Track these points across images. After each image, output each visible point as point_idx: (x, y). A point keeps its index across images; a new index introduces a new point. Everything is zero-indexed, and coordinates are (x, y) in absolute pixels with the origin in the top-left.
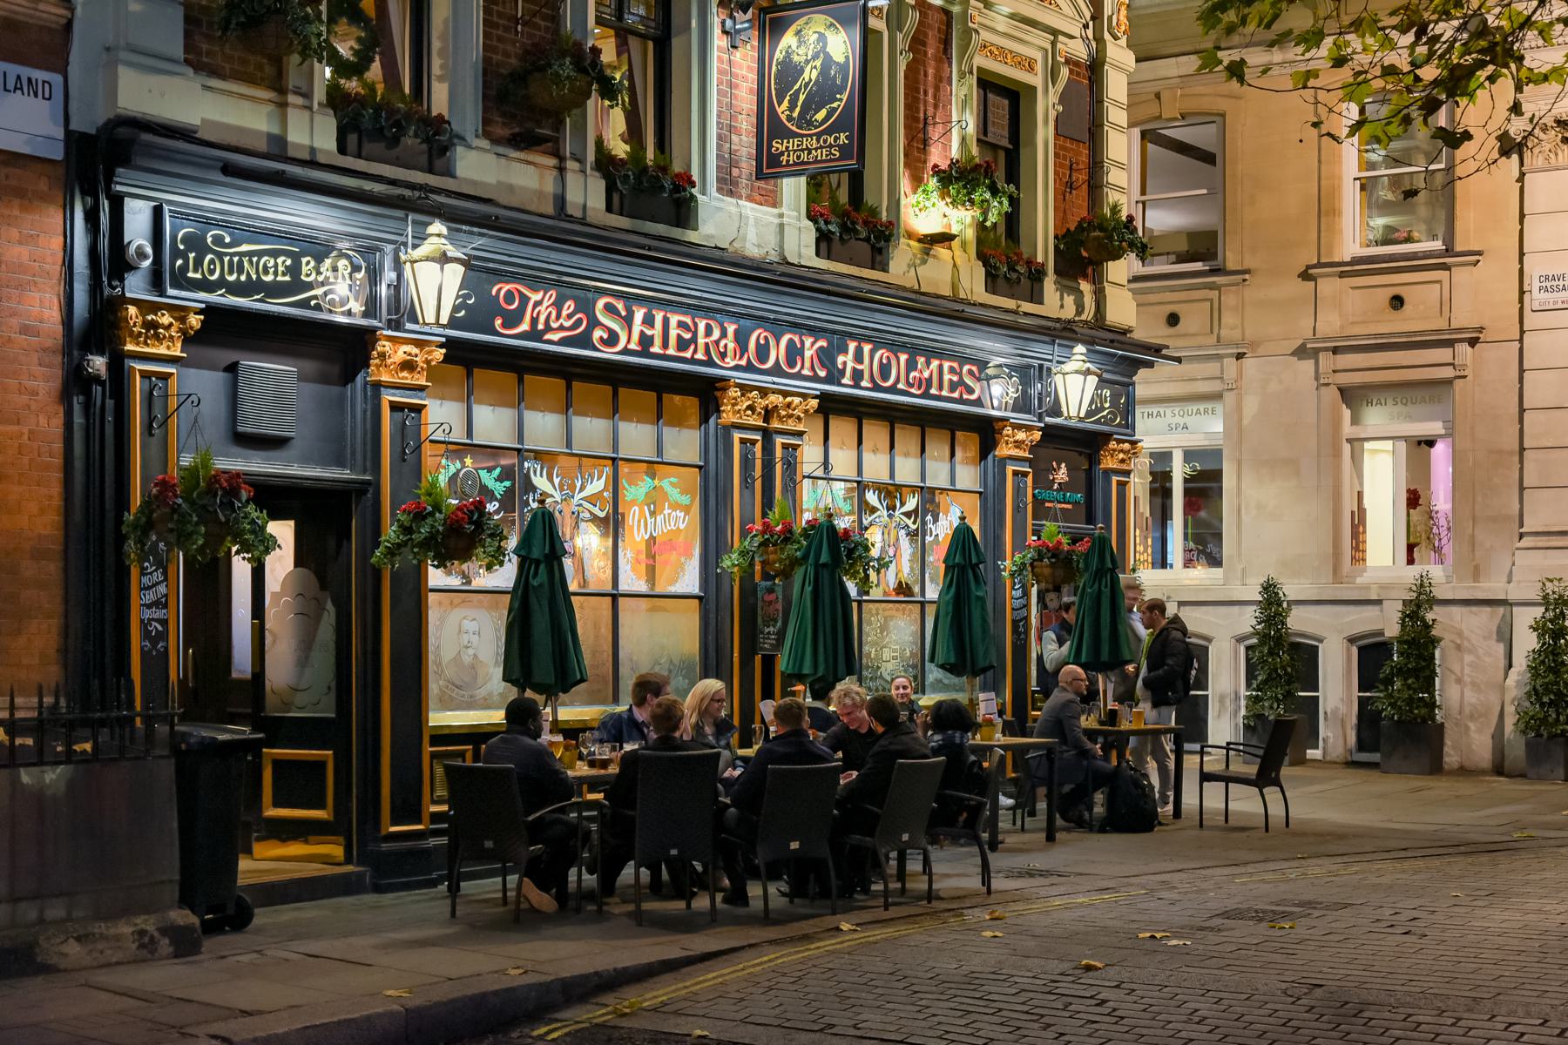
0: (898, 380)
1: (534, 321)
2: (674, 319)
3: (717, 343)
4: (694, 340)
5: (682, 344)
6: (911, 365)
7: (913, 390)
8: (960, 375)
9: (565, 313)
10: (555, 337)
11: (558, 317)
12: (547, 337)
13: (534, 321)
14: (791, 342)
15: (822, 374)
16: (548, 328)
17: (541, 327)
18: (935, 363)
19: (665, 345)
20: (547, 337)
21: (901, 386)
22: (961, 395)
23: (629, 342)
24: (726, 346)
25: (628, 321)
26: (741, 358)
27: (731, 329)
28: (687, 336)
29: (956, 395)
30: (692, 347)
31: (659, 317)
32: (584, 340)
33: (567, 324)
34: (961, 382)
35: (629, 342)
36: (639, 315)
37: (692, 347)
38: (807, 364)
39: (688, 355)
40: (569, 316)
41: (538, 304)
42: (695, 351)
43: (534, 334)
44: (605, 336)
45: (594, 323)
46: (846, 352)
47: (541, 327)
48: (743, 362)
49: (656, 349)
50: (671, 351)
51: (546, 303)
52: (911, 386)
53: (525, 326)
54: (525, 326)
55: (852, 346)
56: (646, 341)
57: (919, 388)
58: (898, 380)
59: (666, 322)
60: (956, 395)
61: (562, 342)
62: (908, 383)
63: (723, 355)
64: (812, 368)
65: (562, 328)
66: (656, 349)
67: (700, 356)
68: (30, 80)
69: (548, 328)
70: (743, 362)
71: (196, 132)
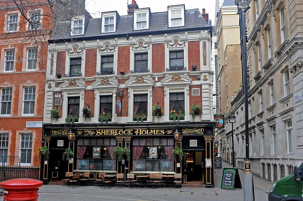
0: (147, 133)
1: (89, 134)
2: (107, 131)
3: (114, 133)
4: (110, 133)
5: (108, 133)
6: (149, 131)
7: (150, 134)
14: (126, 131)
15: (132, 134)
16: (91, 134)
18: (154, 130)
19: (106, 134)
25: (101, 132)
27: (116, 131)
29: (159, 134)
31: (105, 131)
32: (95, 135)
34: (160, 132)
36: (102, 131)
38: (129, 133)
43: (89, 135)
45: (96, 133)
49: (105, 134)
50: (107, 134)
53: (88, 134)
54: (88, 134)
55: (138, 130)
56: (103, 134)
58: (147, 133)
59: (106, 131)
60: (159, 134)
61: (92, 135)
62: (149, 133)
63: (115, 134)
64: (130, 134)
66: (105, 134)
67: (111, 134)
69: (91, 134)
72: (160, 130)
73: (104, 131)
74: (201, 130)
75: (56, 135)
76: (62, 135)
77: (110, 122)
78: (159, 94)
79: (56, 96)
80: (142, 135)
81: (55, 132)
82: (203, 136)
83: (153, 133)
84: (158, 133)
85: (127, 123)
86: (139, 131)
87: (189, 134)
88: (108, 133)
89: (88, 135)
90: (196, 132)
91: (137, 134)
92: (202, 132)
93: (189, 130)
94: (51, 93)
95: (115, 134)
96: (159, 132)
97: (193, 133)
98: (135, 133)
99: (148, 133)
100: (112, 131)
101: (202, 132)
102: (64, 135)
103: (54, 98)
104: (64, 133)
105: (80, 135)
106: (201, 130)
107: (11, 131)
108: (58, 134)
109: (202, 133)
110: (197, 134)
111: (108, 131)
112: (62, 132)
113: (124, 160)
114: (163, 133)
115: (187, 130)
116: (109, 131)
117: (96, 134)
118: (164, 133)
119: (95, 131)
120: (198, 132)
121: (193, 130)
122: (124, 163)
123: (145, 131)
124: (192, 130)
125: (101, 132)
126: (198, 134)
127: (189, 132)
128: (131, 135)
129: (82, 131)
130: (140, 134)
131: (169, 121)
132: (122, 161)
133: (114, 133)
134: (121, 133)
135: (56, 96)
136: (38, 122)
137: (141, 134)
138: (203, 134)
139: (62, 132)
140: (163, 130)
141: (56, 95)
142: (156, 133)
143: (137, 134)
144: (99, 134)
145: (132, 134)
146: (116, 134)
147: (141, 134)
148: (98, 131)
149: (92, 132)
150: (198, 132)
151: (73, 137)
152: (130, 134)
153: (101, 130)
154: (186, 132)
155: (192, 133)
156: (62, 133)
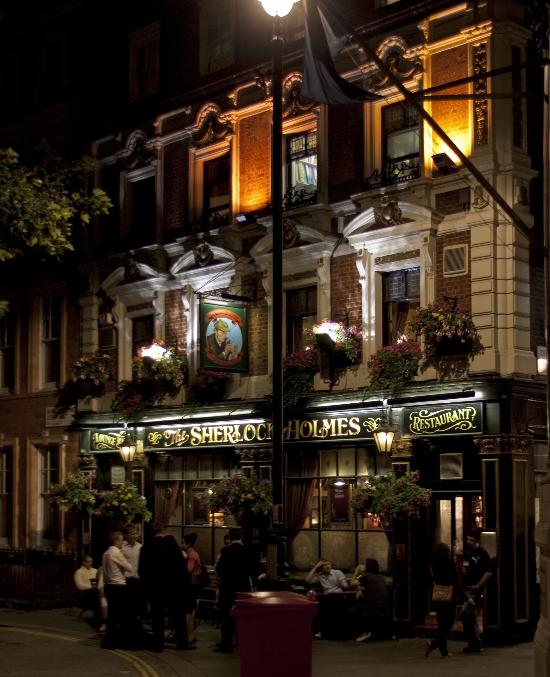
0: (313, 434)
4: (223, 435)
7: (323, 437)
9: (183, 435)
10: (180, 444)
18: (333, 421)
21: (316, 435)
22: (349, 433)
25: (201, 433)
26: (241, 439)
27: (237, 428)
30: (222, 439)
31: (210, 429)
34: (349, 427)
39: (221, 441)
40: (184, 436)
42: (224, 440)
44: (194, 440)
45: (191, 437)
50: (216, 441)
60: (346, 434)
61: (183, 445)
62: (318, 434)
66: (211, 441)
67: (226, 441)
72: (349, 419)
73: (207, 432)
74: (465, 413)
78: (349, 282)
80: (302, 438)
82: (472, 437)
83: (330, 430)
87: (431, 430)
88: (219, 437)
89: (172, 446)
90: (451, 424)
92: (470, 420)
93: (432, 414)
95: (234, 439)
96: (345, 426)
97: (443, 427)
100: (228, 431)
101: (470, 420)
105: (155, 446)
106: (465, 413)
107: (17, 440)
108: (108, 445)
109: (471, 425)
110: (452, 431)
111: (219, 430)
113: (257, 531)
114: (354, 430)
115: (423, 414)
116: (221, 428)
118: (358, 428)
119: (188, 430)
120: (458, 421)
121: (441, 413)
122: (257, 542)
123: (308, 424)
124: (437, 415)
125: (201, 433)
126: (459, 431)
127: (430, 422)
130: (297, 437)
133: (232, 434)
134: (250, 434)
137: (300, 435)
138: (471, 430)
140: (358, 420)
142: (337, 432)
144: (197, 441)
146: (237, 440)
147: (300, 435)
148: (196, 431)
149: (181, 433)
150: (458, 421)
151: (136, 453)
153: (201, 427)
154: (421, 424)
155: (438, 427)
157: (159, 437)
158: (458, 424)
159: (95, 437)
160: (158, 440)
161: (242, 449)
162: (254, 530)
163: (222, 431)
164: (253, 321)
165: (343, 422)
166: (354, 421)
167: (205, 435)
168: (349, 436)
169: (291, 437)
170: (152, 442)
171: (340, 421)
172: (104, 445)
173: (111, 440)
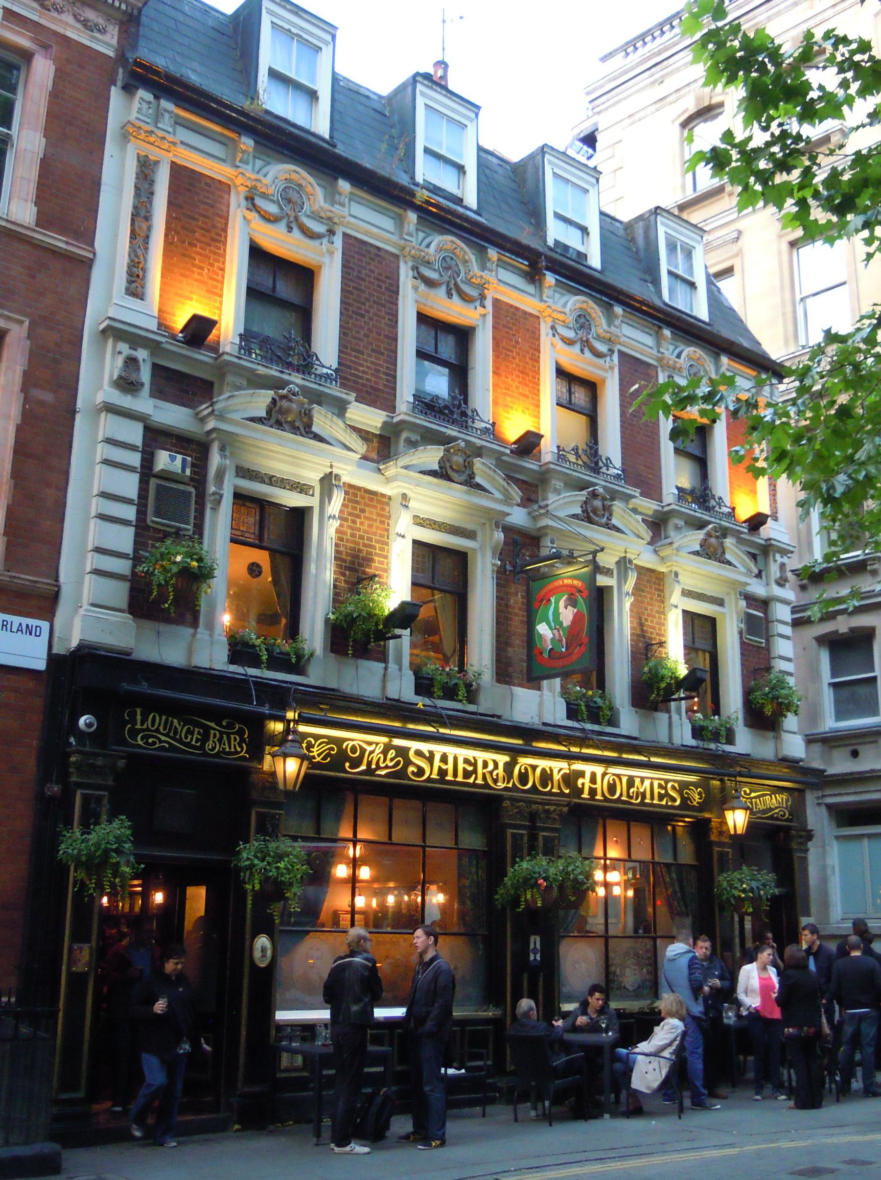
1: (369, 763)
3: (491, 773)
4: (475, 771)
5: (467, 774)
7: (633, 801)
8: (665, 788)
9: (389, 756)
10: (383, 772)
11: (384, 762)
12: (378, 772)
13: (369, 763)
17: (373, 766)
18: (647, 783)
19: (455, 774)
20: (378, 772)
21: (624, 798)
23: (431, 774)
24: (497, 775)
25: (430, 759)
26: (508, 783)
28: (470, 768)
29: (664, 803)
30: (474, 776)
33: (391, 764)
34: (667, 794)
35: (431, 774)
37: (474, 776)
39: (471, 780)
40: (392, 760)
41: (372, 752)
42: (476, 779)
43: (369, 771)
45: (409, 762)
46: (584, 777)
47: (373, 766)
48: (510, 785)
49: (449, 778)
50: (460, 779)
51: (377, 751)
52: (631, 798)
53: (363, 767)
54: (363, 767)
56: (442, 773)
57: (637, 799)
58: (621, 795)
59: (456, 759)
60: (664, 803)
61: (387, 775)
62: (628, 796)
63: (495, 781)
64: (560, 788)
65: (387, 767)
66: (449, 778)
67: (480, 781)
68: (27, 626)
69: (378, 767)
70: (510, 785)
71: (129, 654)
75: (162, 748)
76: (205, 754)
77: (472, 708)
79: (164, 460)
80: (606, 799)
81: (157, 720)
83: (644, 795)
84: (661, 797)
85: (544, 724)
86: (593, 780)
88: (467, 774)
89: (358, 773)
90: (771, 809)
91: (585, 795)
92: (786, 808)
93: (753, 795)
94: (134, 434)
98: (580, 786)
99: (625, 793)
100: (485, 764)
102: (217, 755)
103: (147, 470)
104: (220, 740)
109: (787, 815)
110: (772, 818)
112: (207, 729)
113: (538, 939)
117: (405, 767)
120: (777, 808)
122: (538, 957)
126: (777, 819)
127: (751, 803)
128: (562, 794)
129: (332, 740)
130: (599, 797)
131: (693, 742)
132: (532, 946)
135: (164, 460)
136: (16, 620)
139: (207, 729)
140: (676, 785)
141: (173, 459)
142: (652, 798)
143: (585, 795)
144: (421, 771)
145: (567, 791)
147: (603, 795)
150: (777, 808)
152: (560, 788)
156: (205, 738)
157: (333, 749)
158: (777, 811)
159: (133, 715)
160: (328, 755)
161: (513, 800)
162: (532, 938)
163: (475, 765)
164: (512, 601)
165: (660, 786)
166: (673, 787)
167: (437, 763)
168: (667, 806)
169: (589, 794)
170: (314, 757)
171: (656, 783)
172: (163, 738)
173: (189, 732)
